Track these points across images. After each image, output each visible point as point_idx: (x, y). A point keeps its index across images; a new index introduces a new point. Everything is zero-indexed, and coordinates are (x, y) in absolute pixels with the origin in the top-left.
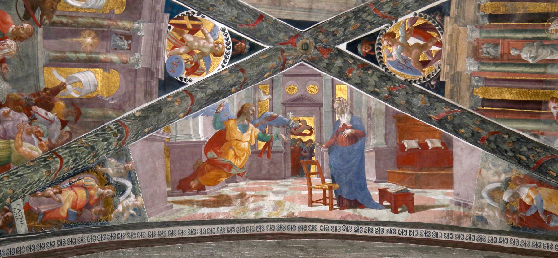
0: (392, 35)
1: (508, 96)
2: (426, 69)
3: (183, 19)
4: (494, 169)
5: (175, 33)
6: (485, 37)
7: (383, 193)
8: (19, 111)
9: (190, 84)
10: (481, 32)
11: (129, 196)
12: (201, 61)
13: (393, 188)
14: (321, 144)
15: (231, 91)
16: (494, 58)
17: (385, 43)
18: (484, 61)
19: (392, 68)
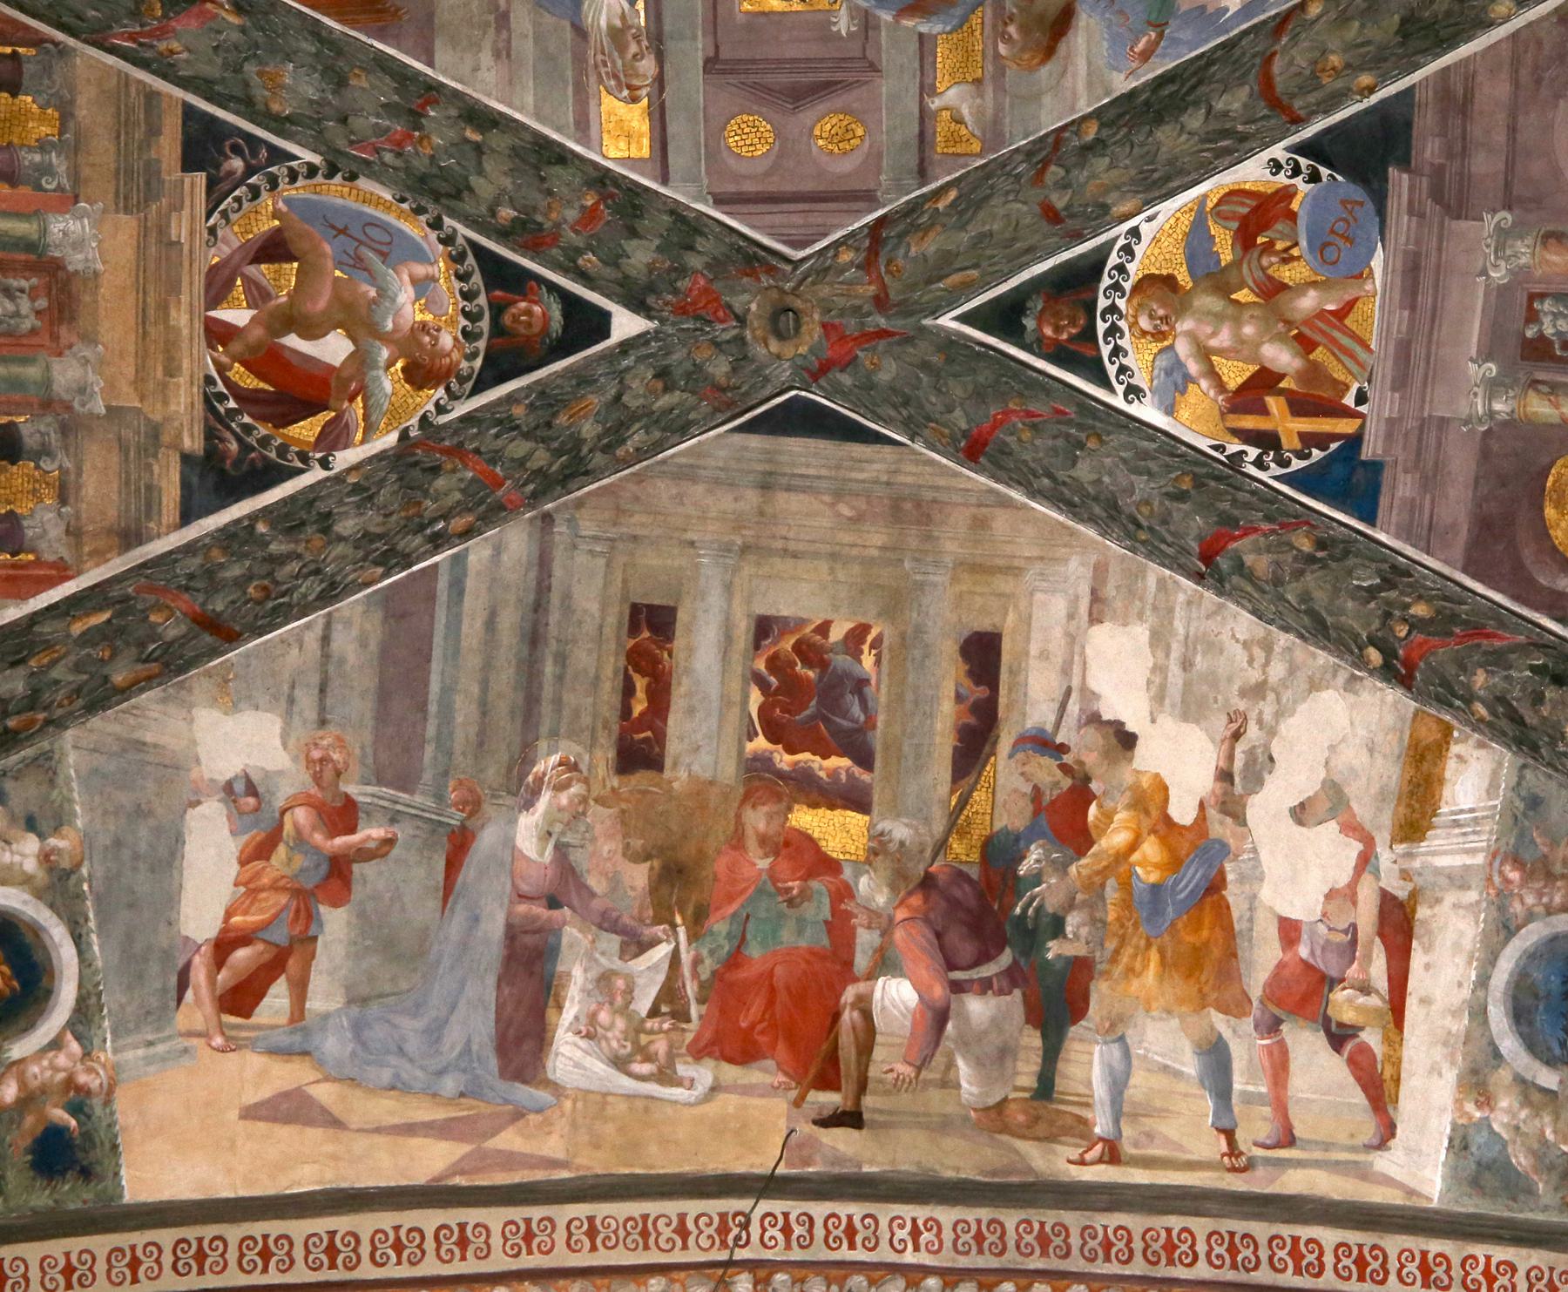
0: (419, 374)
2: (268, 225)
3: (1303, 436)
5: (1339, 375)
6: (25, 361)
9: (1278, 151)
10: (47, 383)
12: (1227, 257)
15: (1102, 125)
17: (446, 341)
18: (22, 257)
19: (414, 229)
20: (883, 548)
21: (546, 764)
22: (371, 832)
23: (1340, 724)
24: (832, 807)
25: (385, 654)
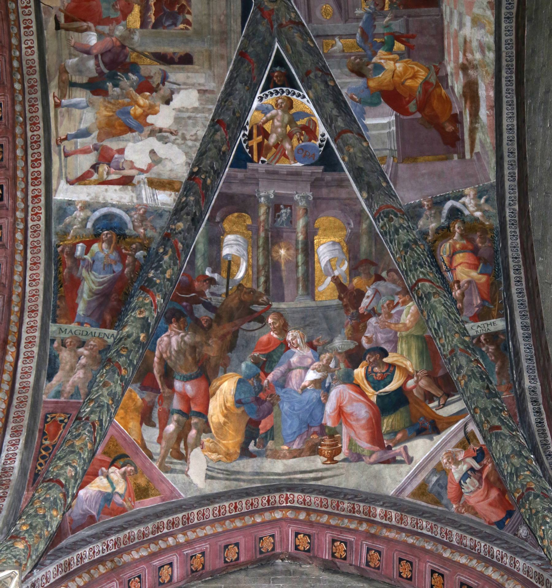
3: (252, 146)
5: (269, 155)
8: (365, 327)
9: (327, 136)
11: (464, 204)
12: (299, 123)
15: (333, 87)
23: (177, 161)
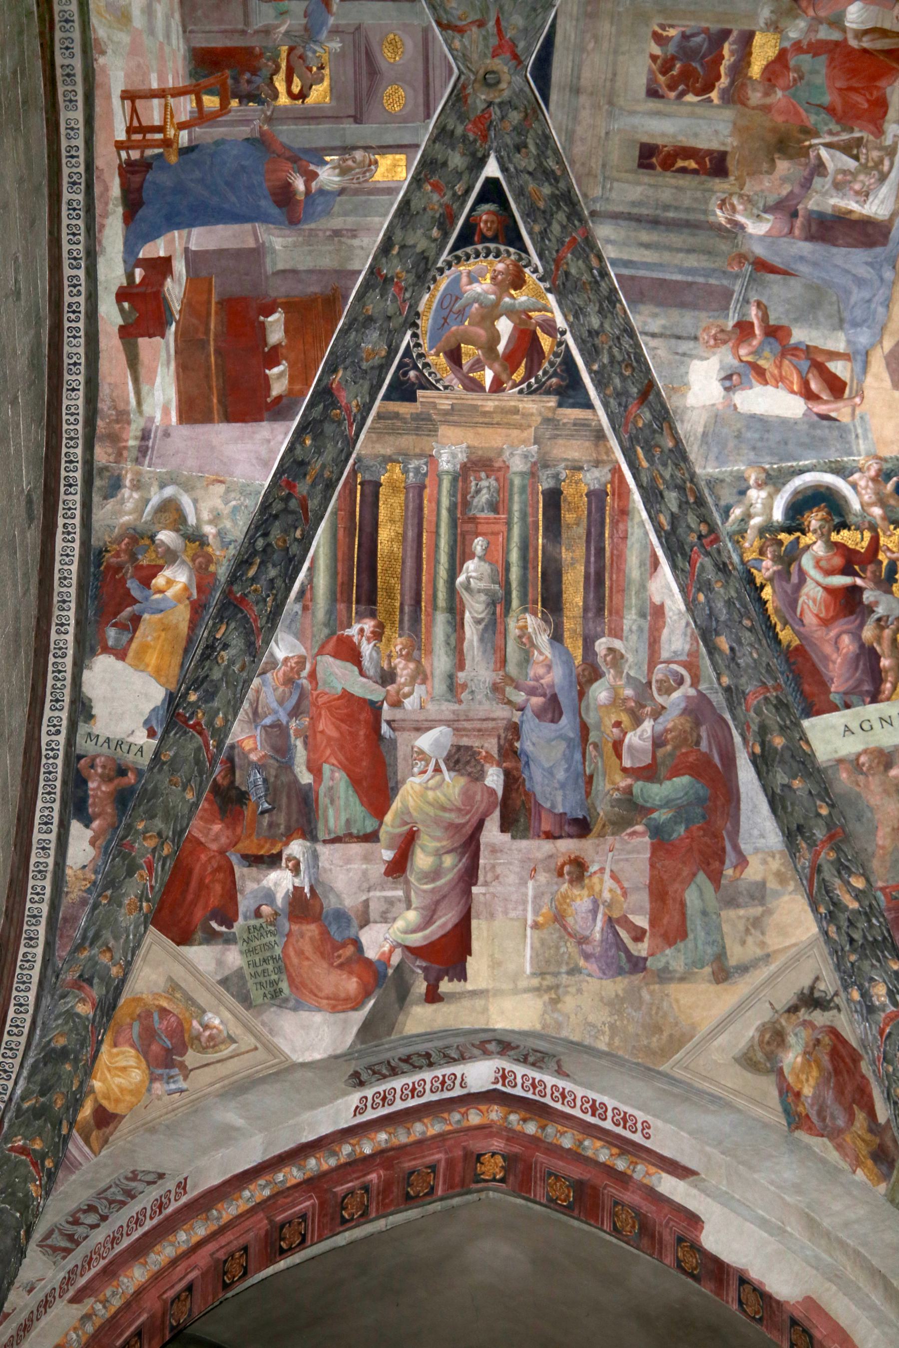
0: (518, 282)
1: (385, 535)
2: (442, 359)
4: (226, 510)
6: (512, 484)
7: (161, 268)
10: (522, 474)
13: (175, 290)
14: (269, 120)
16: (466, 504)
17: (500, 266)
18: (460, 484)
19: (444, 283)
20: (612, 24)
21: (721, 217)
22: (753, 314)
24: (750, 54)
25: (661, 303)
